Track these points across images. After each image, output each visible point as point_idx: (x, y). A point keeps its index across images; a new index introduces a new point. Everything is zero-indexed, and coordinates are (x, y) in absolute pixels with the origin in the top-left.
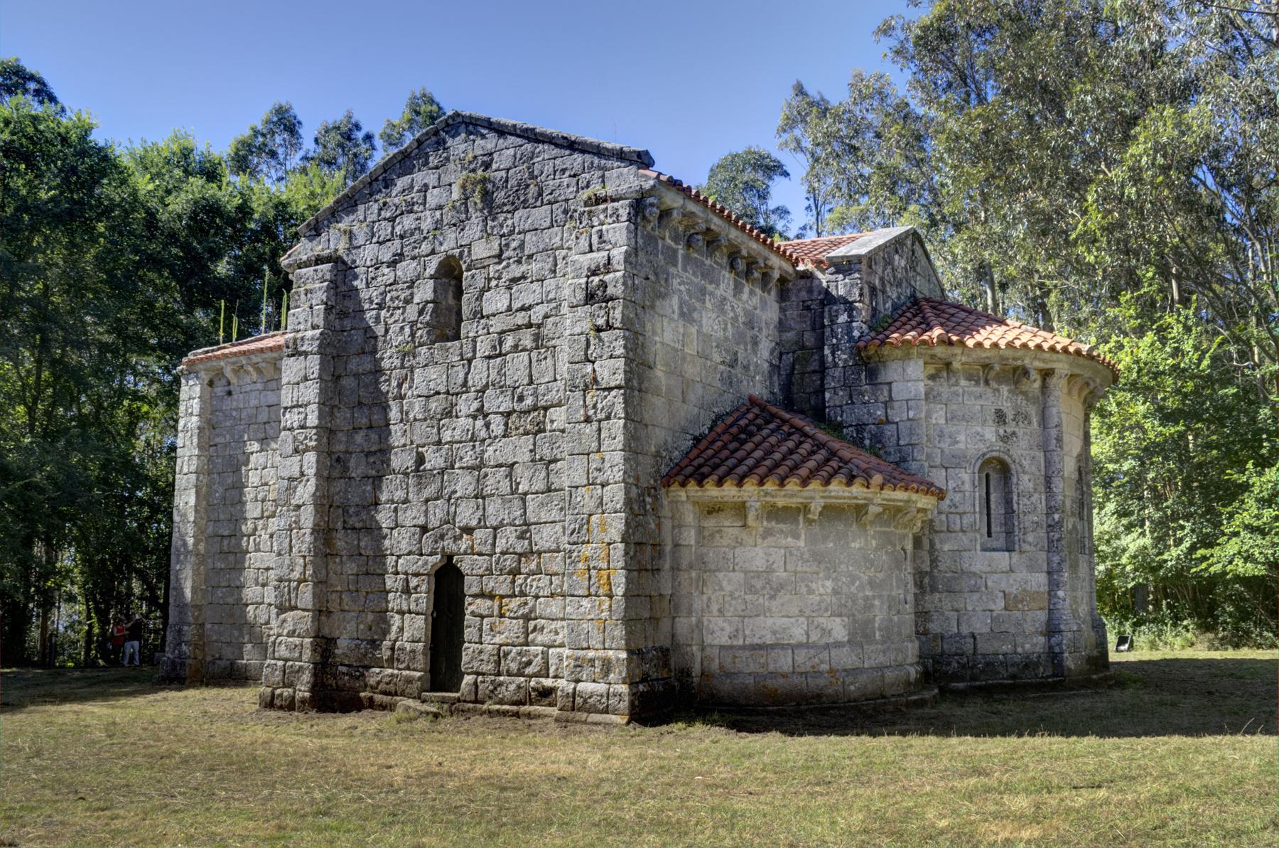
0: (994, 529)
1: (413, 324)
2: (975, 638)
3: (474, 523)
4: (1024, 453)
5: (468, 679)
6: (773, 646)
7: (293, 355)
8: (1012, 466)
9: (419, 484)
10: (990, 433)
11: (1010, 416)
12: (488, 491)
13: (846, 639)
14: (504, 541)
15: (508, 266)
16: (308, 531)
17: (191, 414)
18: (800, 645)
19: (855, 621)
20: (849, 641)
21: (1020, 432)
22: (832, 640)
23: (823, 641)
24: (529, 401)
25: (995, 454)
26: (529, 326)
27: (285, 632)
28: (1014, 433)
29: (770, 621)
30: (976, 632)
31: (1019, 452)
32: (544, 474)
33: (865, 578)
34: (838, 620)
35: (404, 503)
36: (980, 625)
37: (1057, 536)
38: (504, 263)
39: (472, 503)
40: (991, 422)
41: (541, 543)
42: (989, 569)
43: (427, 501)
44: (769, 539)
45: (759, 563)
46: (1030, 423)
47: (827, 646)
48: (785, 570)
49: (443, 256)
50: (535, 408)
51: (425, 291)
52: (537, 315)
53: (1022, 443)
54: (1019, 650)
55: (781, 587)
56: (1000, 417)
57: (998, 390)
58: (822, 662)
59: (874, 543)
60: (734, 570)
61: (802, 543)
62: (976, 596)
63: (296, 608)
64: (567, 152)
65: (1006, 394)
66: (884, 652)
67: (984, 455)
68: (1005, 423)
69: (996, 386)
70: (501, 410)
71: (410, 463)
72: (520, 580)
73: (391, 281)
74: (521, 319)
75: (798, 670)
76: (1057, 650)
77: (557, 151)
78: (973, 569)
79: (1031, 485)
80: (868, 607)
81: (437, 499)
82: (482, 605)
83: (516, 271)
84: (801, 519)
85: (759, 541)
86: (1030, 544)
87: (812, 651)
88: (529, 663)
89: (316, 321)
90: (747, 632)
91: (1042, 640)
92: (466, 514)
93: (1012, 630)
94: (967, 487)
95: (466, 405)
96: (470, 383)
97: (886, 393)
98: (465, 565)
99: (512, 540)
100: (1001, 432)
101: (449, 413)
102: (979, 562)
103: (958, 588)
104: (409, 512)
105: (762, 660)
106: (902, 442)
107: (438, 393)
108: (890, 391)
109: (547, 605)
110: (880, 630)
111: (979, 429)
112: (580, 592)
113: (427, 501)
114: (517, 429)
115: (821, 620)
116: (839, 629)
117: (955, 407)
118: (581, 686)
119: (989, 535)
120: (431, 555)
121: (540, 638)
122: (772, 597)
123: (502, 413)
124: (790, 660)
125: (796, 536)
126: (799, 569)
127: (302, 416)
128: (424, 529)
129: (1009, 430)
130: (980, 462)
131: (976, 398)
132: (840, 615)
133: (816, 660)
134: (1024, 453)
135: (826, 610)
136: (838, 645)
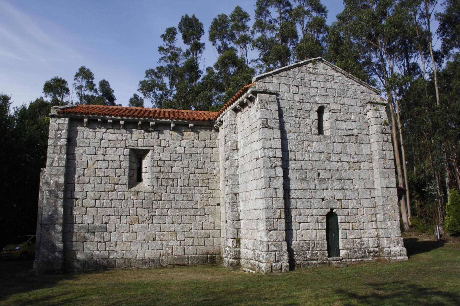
1: (311, 126)
3: (342, 198)
5: (342, 253)
7: (266, 127)
9: (320, 183)
12: (346, 187)
14: (353, 204)
15: (344, 114)
16: (281, 199)
17: (60, 137)
24: (356, 160)
26: (353, 135)
27: (272, 240)
32: (363, 183)
35: (315, 189)
38: (342, 113)
39: (341, 191)
41: (364, 205)
43: (323, 189)
49: (320, 105)
50: (358, 162)
51: (315, 115)
52: (355, 132)
63: (277, 230)
64: (359, 84)
70: (347, 161)
71: (316, 176)
72: (358, 217)
73: (300, 108)
74: (350, 132)
77: (355, 83)
81: (327, 189)
82: (346, 226)
83: (347, 116)
88: (364, 244)
89: (274, 116)
92: (339, 195)
95: (334, 158)
96: (335, 150)
98: (339, 212)
99: (355, 204)
101: (328, 160)
104: (317, 193)
107: (324, 152)
109: (368, 225)
112: (388, 220)
113: (323, 189)
114: (353, 168)
118: (391, 249)
120: (327, 208)
121: (366, 236)
123: (347, 162)
127: (274, 152)
128: (323, 199)
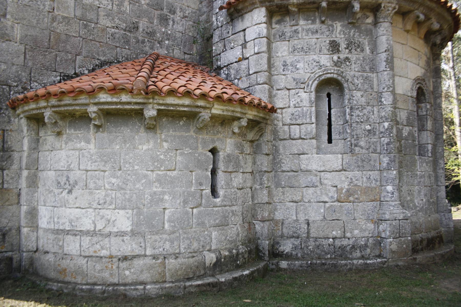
0: (333, 137)
2: (308, 224)
4: (357, 74)
6: (68, 232)
8: (345, 85)
10: (326, 60)
11: (343, 46)
13: (129, 229)
18: (87, 233)
19: (139, 213)
20: (132, 231)
21: (353, 57)
22: (115, 230)
23: (107, 230)
25: (329, 76)
28: (347, 59)
29: (68, 211)
30: (311, 219)
31: (352, 73)
33: (153, 176)
34: (122, 212)
36: (315, 214)
37: (386, 140)
40: (326, 52)
42: (322, 169)
44: (70, 144)
45: (62, 164)
46: (362, 51)
47: (109, 235)
48: (79, 169)
53: (353, 66)
54: (348, 235)
55: (76, 183)
56: (334, 47)
57: (332, 26)
58: (102, 248)
59: (165, 145)
60: (50, 170)
61: (92, 146)
62: (311, 190)
65: (339, 28)
66: (172, 242)
67: (320, 76)
68: (338, 51)
69: (330, 23)
75: (83, 254)
76: (383, 235)
78: (309, 168)
79: (363, 99)
80: (157, 199)
84: (92, 127)
85: (64, 146)
86: (362, 148)
87: (95, 239)
90: (56, 220)
91: (371, 226)
93: (344, 218)
94: (306, 103)
97: (242, 38)
100: (335, 58)
102: (313, 162)
103: (297, 184)
105: (61, 243)
106: (251, 72)
108: (245, 36)
110: (169, 221)
111: (315, 57)
115: (108, 212)
116: (123, 221)
117: (296, 42)
119: (330, 141)
122: (70, 192)
124: (78, 245)
125: (88, 142)
126: (89, 168)
129: (342, 56)
130: (316, 82)
131: (313, 33)
132: (124, 208)
133: (98, 246)
134: (357, 74)
135: (111, 204)
136: (121, 234)
